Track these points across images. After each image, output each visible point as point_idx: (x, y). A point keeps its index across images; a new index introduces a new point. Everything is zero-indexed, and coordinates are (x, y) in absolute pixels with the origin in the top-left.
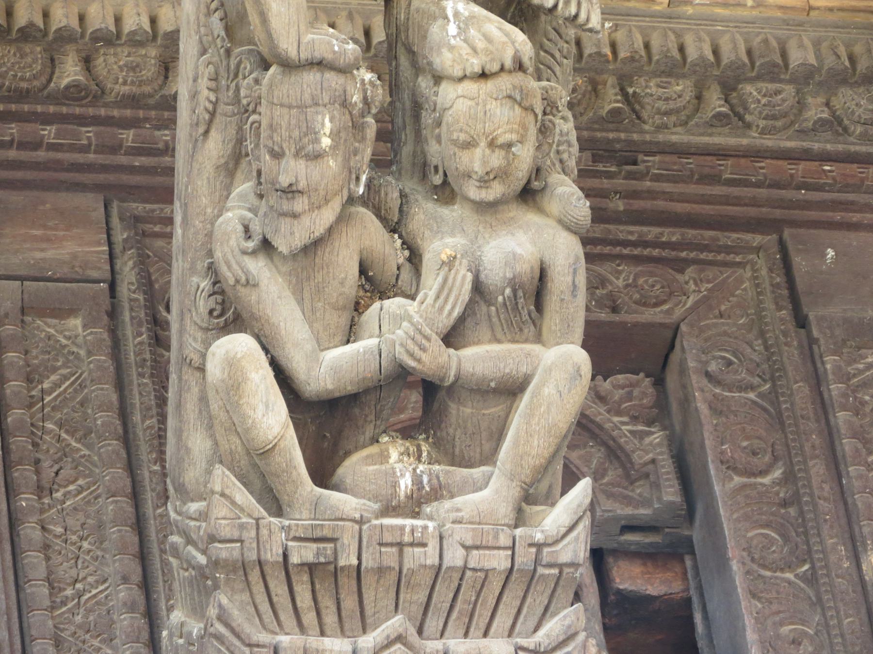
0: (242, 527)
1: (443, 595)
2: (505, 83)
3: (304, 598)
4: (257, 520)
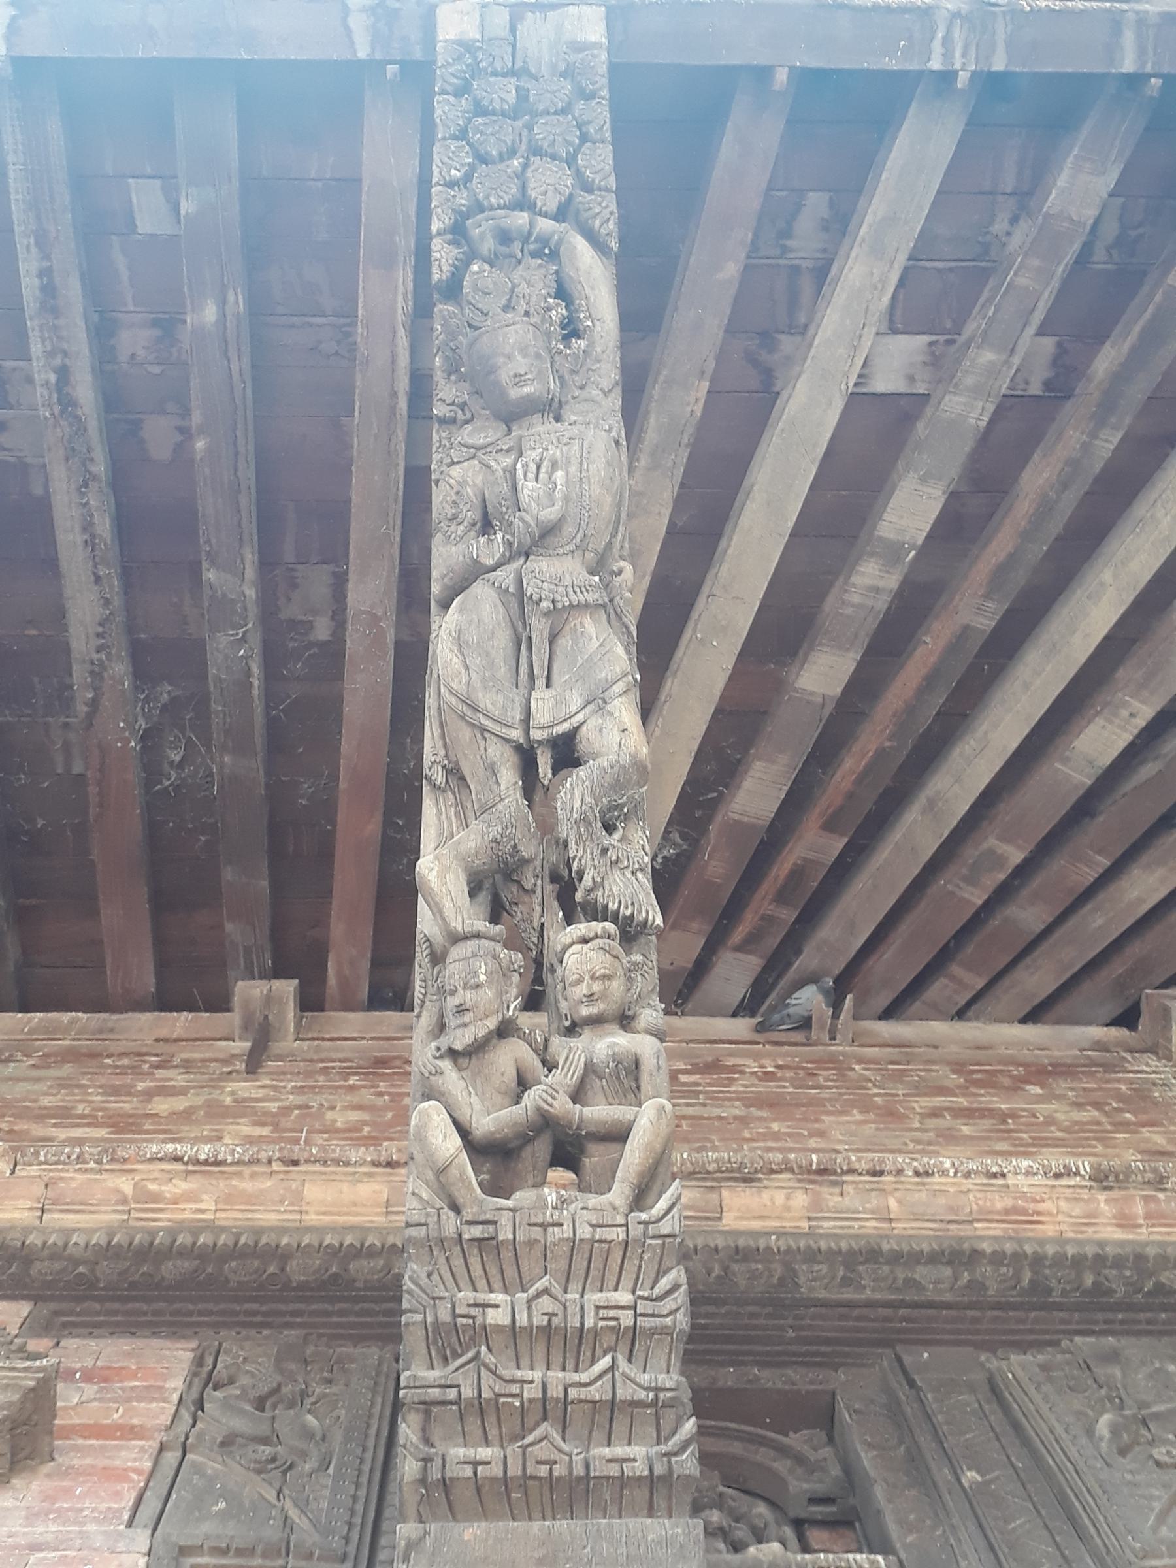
0: (427, 1215)
1: (580, 1264)
2: (598, 942)
3: (477, 1270)
4: (438, 1210)
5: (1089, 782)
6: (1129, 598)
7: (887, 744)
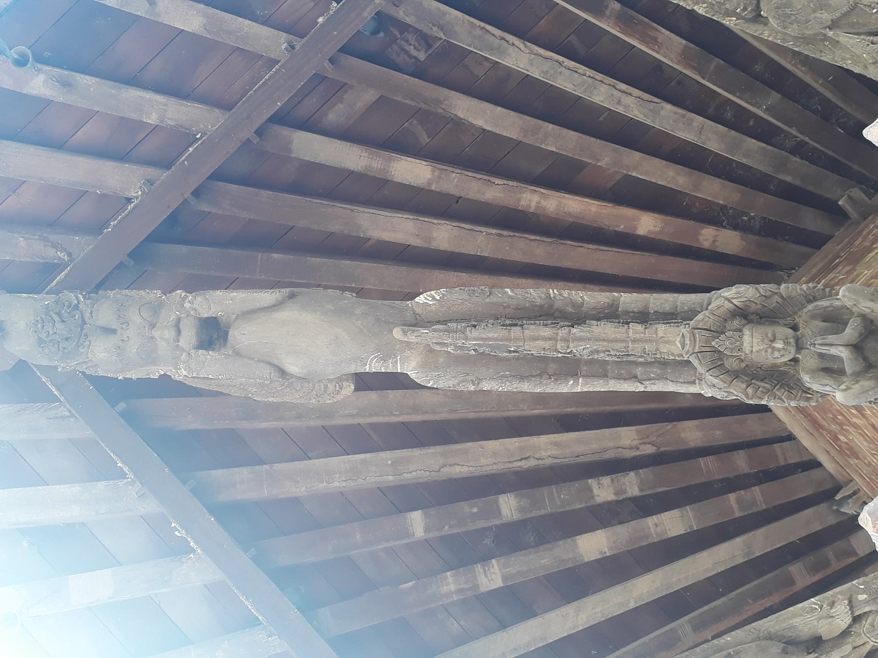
5: (688, 507)
6: (629, 584)
7: (750, 601)
